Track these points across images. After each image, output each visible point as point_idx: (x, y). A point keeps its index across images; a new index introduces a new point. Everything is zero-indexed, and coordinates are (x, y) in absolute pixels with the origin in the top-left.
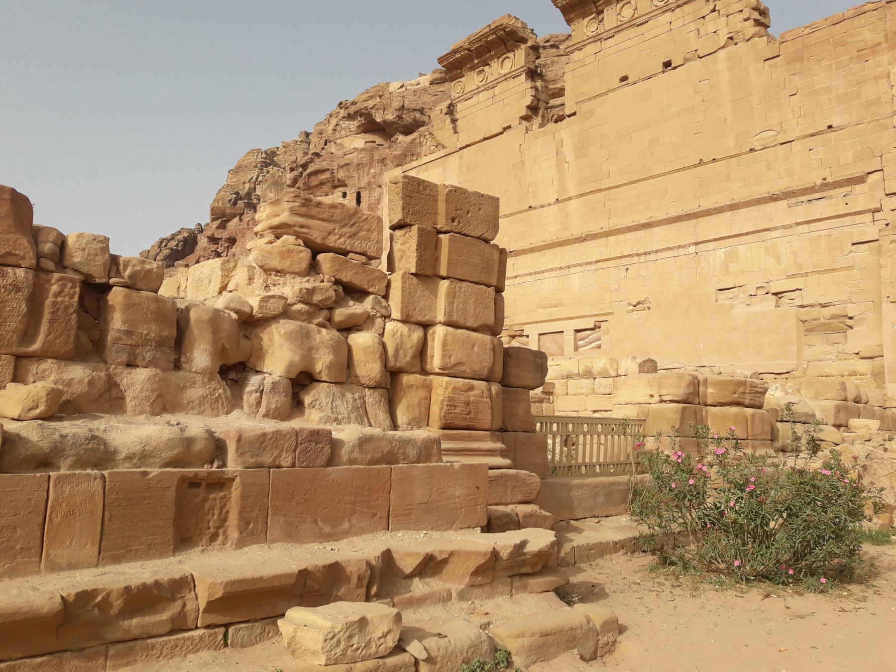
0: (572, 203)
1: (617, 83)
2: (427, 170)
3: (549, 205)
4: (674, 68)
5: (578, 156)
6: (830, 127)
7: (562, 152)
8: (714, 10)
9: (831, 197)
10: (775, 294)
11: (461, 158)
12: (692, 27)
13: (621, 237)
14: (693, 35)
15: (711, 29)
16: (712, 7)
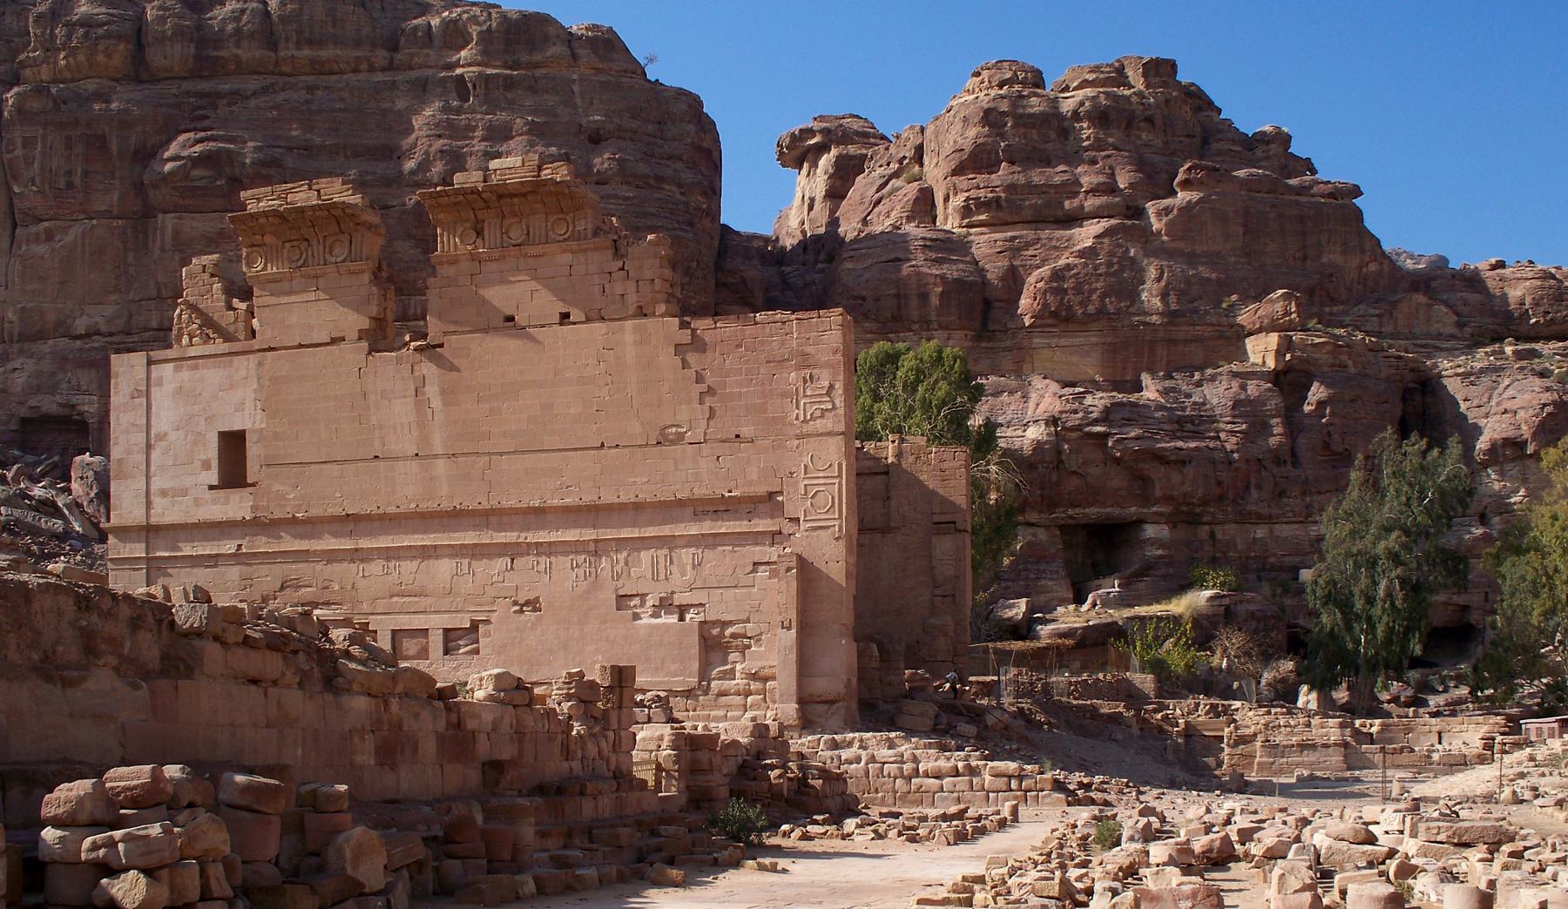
0: (441, 462)
1: (500, 322)
2: (196, 367)
3: (405, 458)
4: (574, 323)
5: (446, 403)
6: (738, 436)
7: (424, 393)
8: (623, 269)
9: (736, 511)
10: (679, 606)
11: (260, 364)
12: (596, 280)
13: (505, 519)
14: (597, 289)
15: (619, 290)
16: (620, 264)
